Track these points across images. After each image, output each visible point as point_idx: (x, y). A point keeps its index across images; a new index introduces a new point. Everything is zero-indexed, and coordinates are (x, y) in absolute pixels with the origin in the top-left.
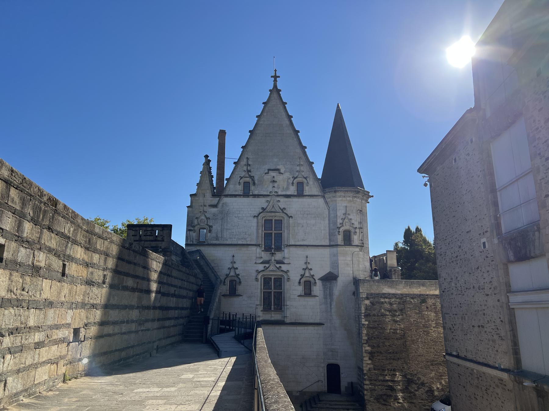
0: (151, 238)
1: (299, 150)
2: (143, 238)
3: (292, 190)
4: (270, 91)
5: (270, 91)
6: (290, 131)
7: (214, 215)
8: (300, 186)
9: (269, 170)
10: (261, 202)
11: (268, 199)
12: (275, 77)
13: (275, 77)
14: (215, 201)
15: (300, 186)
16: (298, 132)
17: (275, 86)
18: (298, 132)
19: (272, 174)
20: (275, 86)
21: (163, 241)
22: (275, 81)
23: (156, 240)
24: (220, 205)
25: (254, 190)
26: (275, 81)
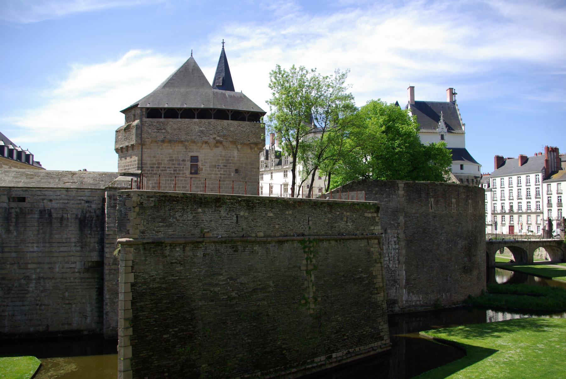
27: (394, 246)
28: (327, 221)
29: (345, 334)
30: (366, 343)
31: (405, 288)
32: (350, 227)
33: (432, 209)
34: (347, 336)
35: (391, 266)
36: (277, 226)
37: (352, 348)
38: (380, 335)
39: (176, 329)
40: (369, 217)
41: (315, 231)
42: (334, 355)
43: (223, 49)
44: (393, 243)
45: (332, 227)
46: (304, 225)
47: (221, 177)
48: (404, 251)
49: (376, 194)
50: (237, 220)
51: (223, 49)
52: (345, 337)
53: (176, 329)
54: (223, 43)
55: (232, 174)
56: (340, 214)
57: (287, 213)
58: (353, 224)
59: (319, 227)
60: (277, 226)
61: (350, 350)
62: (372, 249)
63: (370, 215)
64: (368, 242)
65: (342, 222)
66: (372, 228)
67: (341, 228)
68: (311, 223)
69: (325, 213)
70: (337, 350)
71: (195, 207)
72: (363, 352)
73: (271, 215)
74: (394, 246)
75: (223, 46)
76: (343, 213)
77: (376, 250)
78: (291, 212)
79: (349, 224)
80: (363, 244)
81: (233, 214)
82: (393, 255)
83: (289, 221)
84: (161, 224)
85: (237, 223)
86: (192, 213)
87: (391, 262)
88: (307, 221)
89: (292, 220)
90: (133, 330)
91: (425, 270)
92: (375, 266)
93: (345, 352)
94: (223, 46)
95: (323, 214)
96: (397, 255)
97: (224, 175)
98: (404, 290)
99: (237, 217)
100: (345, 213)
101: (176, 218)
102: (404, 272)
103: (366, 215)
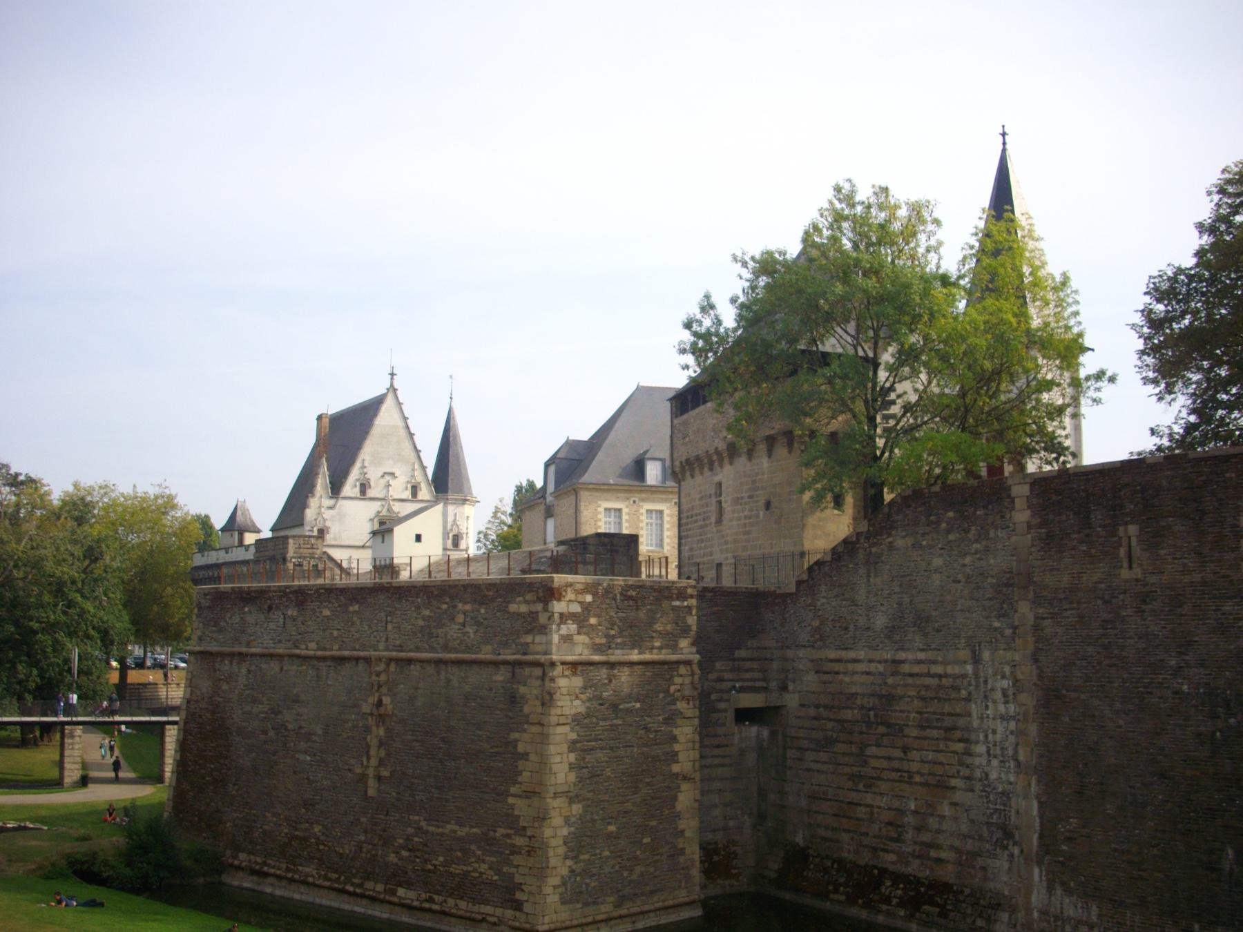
0: (309, 546)
1: (413, 455)
2: (302, 546)
3: (407, 494)
4: (388, 389)
5: (388, 389)
6: (402, 432)
7: (332, 516)
8: (415, 490)
9: (385, 473)
10: (376, 506)
11: (384, 503)
12: (392, 375)
13: (392, 375)
14: (332, 502)
15: (415, 490)
16: (414, 434)
17: (392, 385)
18: (414, 434)
19: (387, 478)
20: (392, 385)
21: (317, 549)
22: (392, 379)
23: (312, 548)
24: (337, 506)
25: (371, 493)
26: (392, 379)
27: (1002, 708)
28: (421, 623)
29: (430, 861)
30: (474, 899)
31: (1039, 864)
32: (472, 636)
33: (1134, 565)
34: (435, 866)
35: (993, 775)
36: (335, 633)
37: (439, 895)
38: (514, 895)
39: (212, 766)
40: (519, 614)
41: (398, 642)
42: (401, 892)
43: (1004, 150)
44: (998, 695)
45: (431, 635)
46: (377, 631)
47: (745, 525)
48: (1033, 729)
49: (948, 532)
50: (284, 623)
51: (1004, 150)
52: (429, 867)
53: (212, 766)
54: (1004, 135)
55: (761, 513)
56: (449, 608)
57: (351, 609)
58: (477, 630)
59: (404, 635)
60: (335, 633)
61: (436, 897)
62: (522, 689)
63: (524, 608)
64: (513, 673)
65: (453, 626)
66: (529, 639)
67: (449, 637)
68: (390, 627)
69: (418, 608)
70: (409, 885)
71: (242, 605)
72: (461, 913)
73: (327, 612)
74: (1002, 708)
75: (1004, 144)
76: (455, 607)
77: (535, 692)
78: (356, 607)
79: (468, 629)
80: (501, 676)
81: (280, 613)
82: (998, 737)
83: (353, 623)
84: (214, 628)
85: (284, 627)
86: (239, 614)
87: (995, 762)
88: (384, 624)
89: (358, 623)
90: (181, 756)
91: (1110, 809)
92: (525, 731)
93: (423, 896)
94: (1004, 144)
95: (413, 609)
96: (1012, 739)
97: (750, 518)
98: (1036, 871)
99: (285, 618)
100: (460, 605)
101: (226, 621)
102: (1035, 804)
103: (513, 608)
